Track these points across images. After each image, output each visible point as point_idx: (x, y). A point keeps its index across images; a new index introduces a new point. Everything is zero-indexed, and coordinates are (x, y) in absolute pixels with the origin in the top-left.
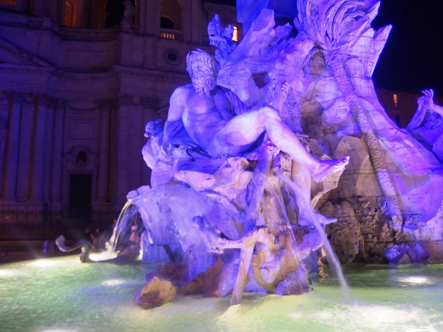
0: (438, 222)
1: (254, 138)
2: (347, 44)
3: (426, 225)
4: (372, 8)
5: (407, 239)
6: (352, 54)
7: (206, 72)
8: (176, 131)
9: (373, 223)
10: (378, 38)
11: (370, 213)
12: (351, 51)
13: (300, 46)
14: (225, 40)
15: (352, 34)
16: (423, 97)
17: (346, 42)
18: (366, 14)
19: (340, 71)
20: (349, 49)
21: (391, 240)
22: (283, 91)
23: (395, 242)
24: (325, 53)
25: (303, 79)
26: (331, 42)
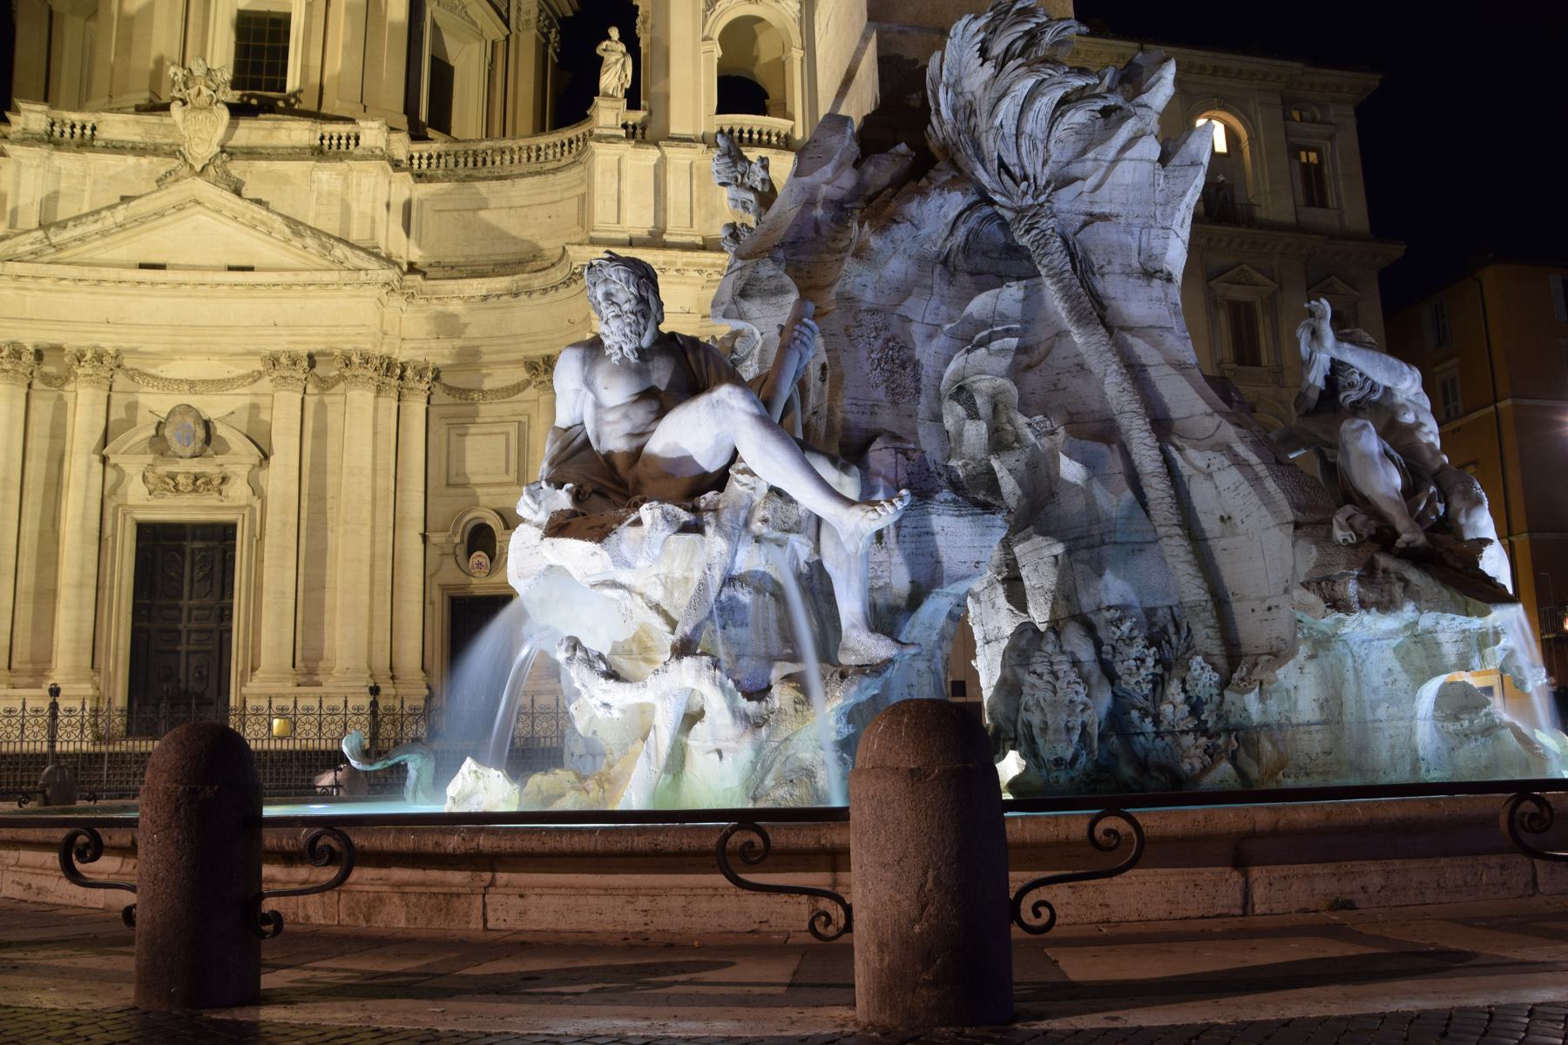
0: (1306, 670)
1: (715, 457)
2: (1079, 183)
3: (1277, 680)
4: (1153, 79)
5: (1232, 720)
6: (1096, 209)
7: (626, 307)
8: (569, 449)
9: (1140, 679)
10: (1176, 161)
11: (1134, 651)
12: (1092, 203)
13: (913, 208)
14: (751, 196)
15: (1090, 155)
16: (1311, 320)
17: (1076, 179)
18: (1129, 100)
19: (1051, 262)
20: (1085, 197)
21: (1191, 726)
22: (796, 339)
23: (1201, 729)
24: (1009, 215)
25: (946, 292)
26: (1018, 185)
